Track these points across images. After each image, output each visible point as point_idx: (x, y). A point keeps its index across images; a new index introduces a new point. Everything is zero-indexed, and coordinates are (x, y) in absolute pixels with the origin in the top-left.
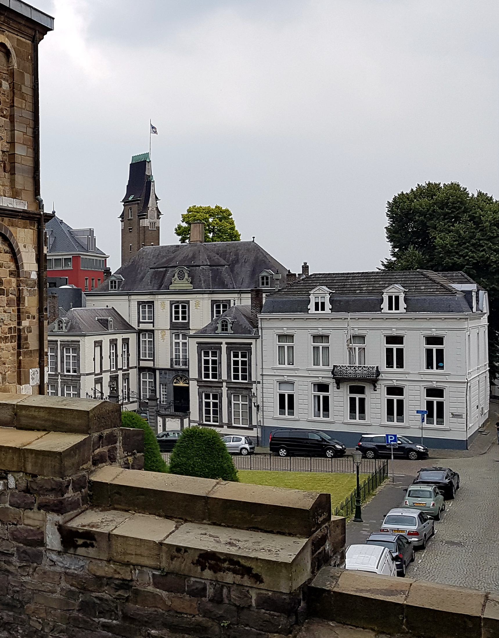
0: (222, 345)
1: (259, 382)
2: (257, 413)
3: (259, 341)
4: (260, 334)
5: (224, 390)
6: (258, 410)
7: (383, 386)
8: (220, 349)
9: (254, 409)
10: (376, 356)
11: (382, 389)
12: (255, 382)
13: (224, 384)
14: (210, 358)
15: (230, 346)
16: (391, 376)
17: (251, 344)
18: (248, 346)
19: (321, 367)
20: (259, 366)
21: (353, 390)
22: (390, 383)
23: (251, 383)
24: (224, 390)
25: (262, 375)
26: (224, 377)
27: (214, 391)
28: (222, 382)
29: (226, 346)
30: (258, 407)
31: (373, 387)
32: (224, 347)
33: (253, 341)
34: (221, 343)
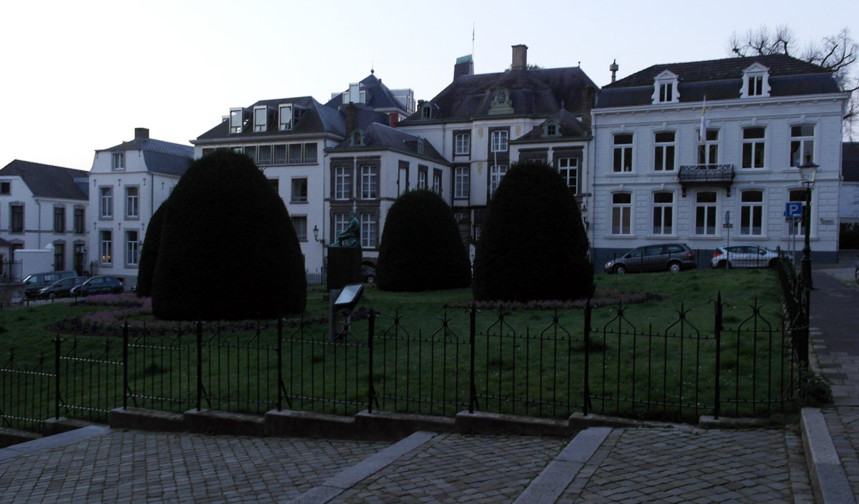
1: (590, 195)
3: (592, 143)
10: (730, 153)
12: (585, 195)
16: (750, 177)
17: (582, 147)
18: (578, 150)
19: (664, 171)
20: (592, 175)
22: (745, 186)
25: (595, 185)
33: (585, 144)
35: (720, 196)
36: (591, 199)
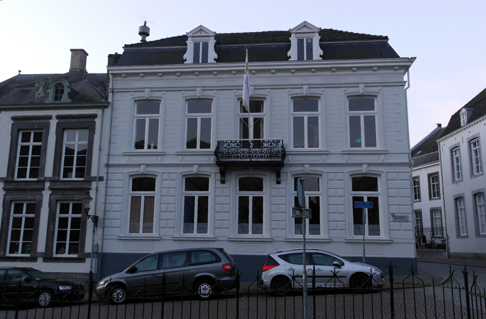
0: (50, 121)
1: (101, 179)
2: (94, 232)
3: (108, 111)
4: (110, 100)
5: (46, 195)
6: (96, 225)
7: (289, 175)
8: (47, 127)
9: (90, 223)
11: (288, 182)
12: (94, 179)
13: (47, 185)
14: (31, 144)
15: (63, 121)
17: (95, 116)
18: (91, 120)
20: (105, 152)
21: (244, 185)
23: (89, 181)
24: (46, 195)
26: (49, 172)
27: (30, 196)
28: (44, 182)
29: (57, 121)
30: (95, 219)
31: (274, 178)
32: (53, 124)
33: (98, 112)
34: (50, 118)
35: (268, 182)
36: (102, 184)
